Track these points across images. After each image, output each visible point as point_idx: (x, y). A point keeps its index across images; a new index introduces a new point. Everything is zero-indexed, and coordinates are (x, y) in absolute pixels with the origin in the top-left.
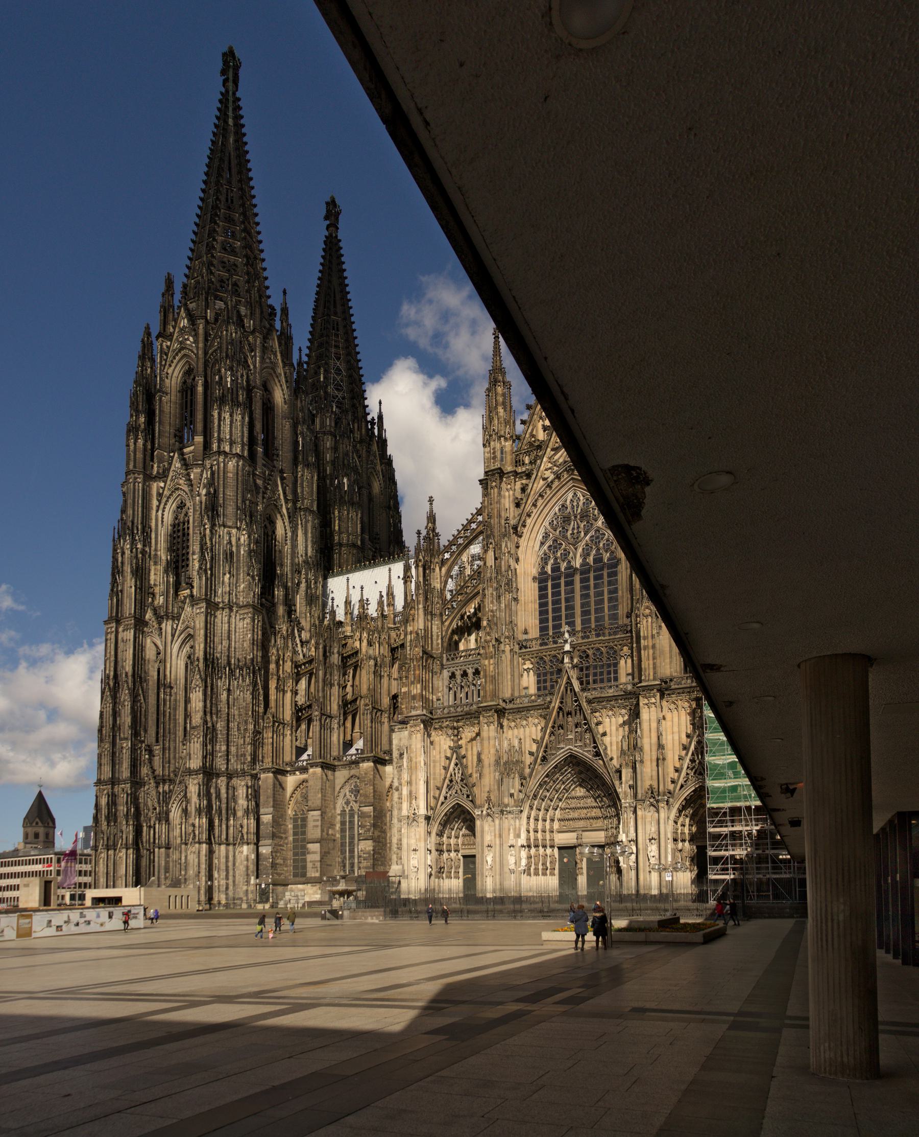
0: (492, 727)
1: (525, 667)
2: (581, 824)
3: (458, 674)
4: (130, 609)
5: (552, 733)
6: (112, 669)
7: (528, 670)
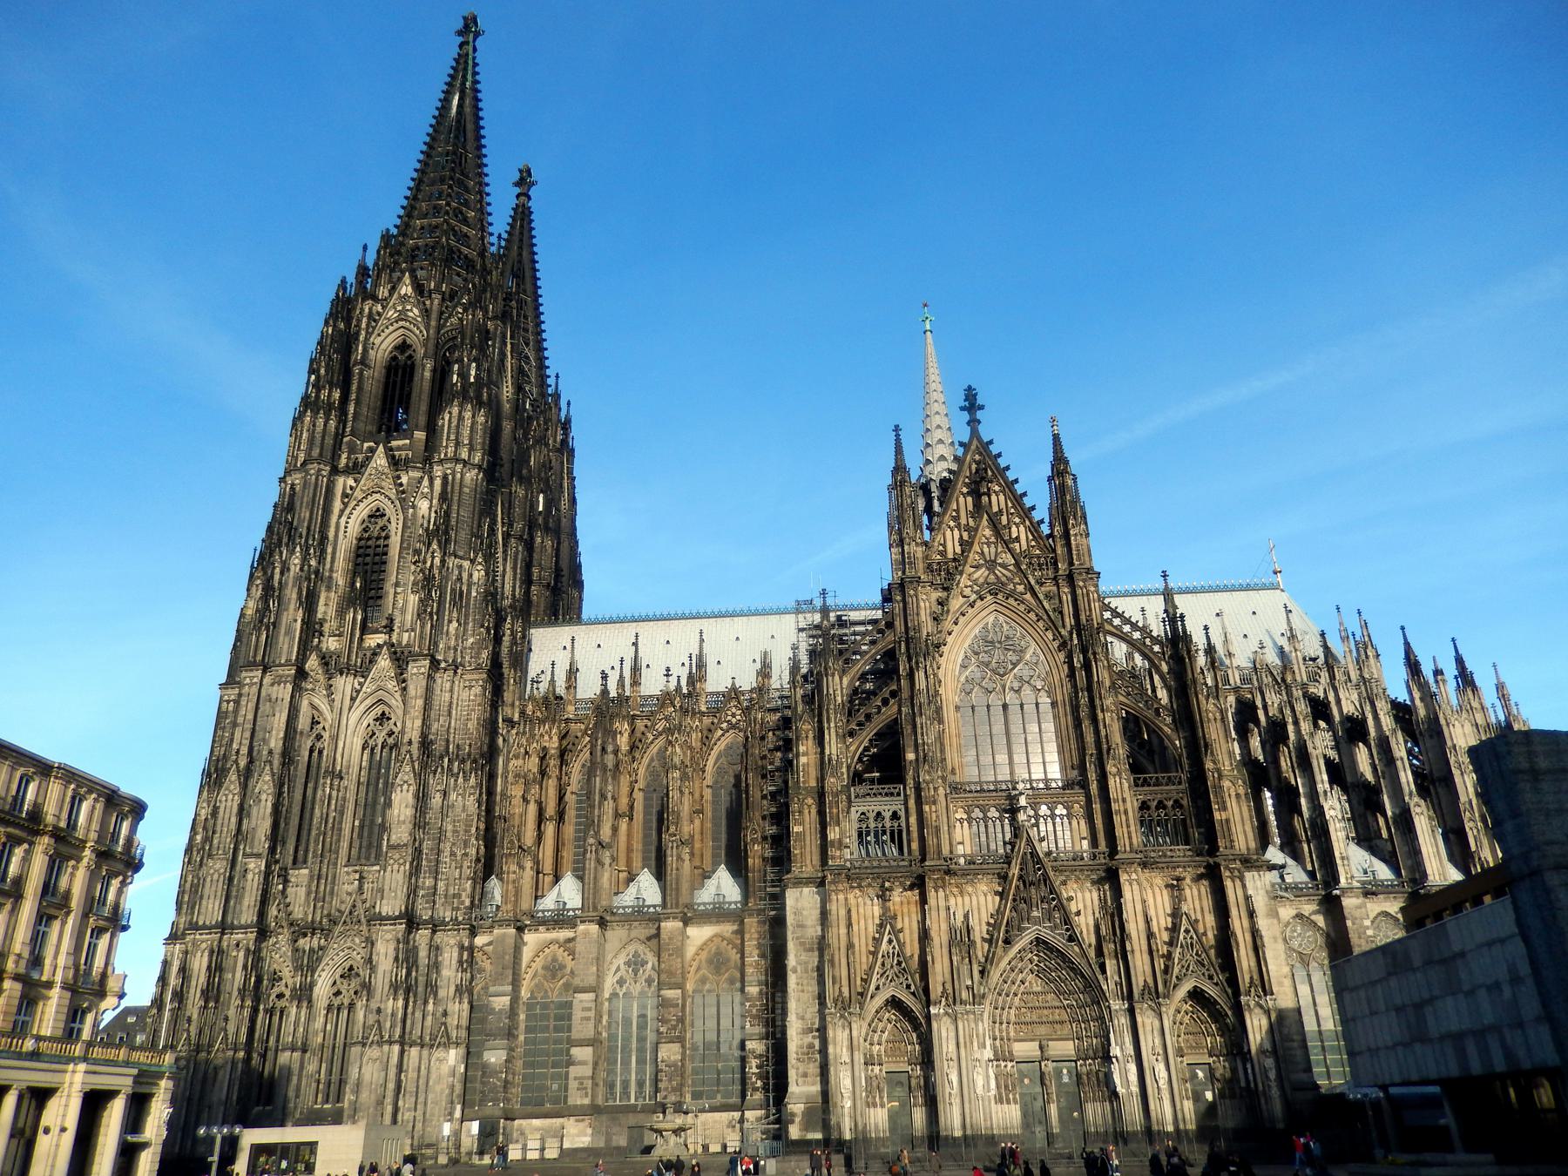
0: (941, 893)
1: (958, 816)
2: (1042, 1030)
3: (872, 815)
4: (290, 653)
5: (1014, 908)
6: (247, 742)
7: (961, 821)
